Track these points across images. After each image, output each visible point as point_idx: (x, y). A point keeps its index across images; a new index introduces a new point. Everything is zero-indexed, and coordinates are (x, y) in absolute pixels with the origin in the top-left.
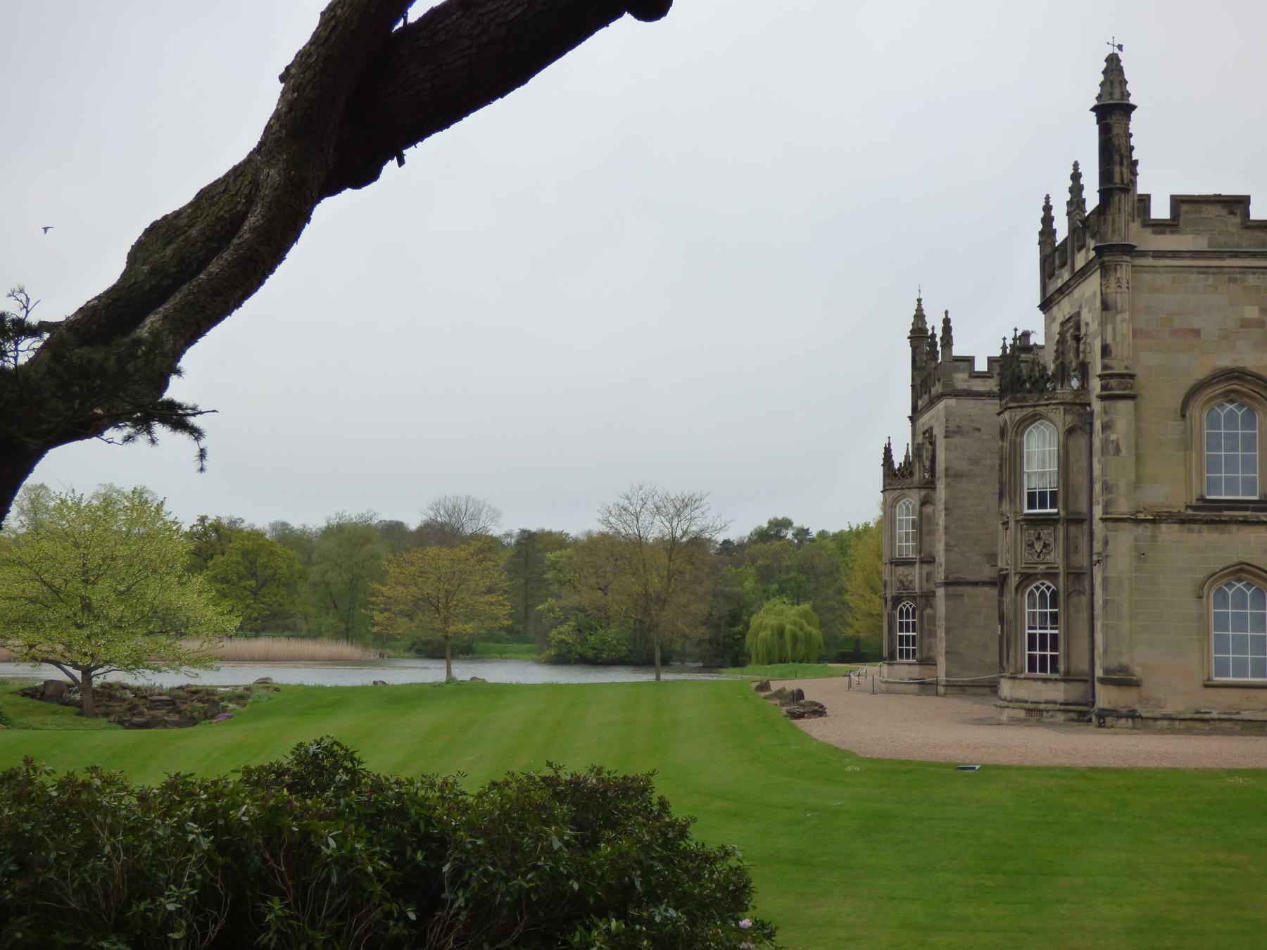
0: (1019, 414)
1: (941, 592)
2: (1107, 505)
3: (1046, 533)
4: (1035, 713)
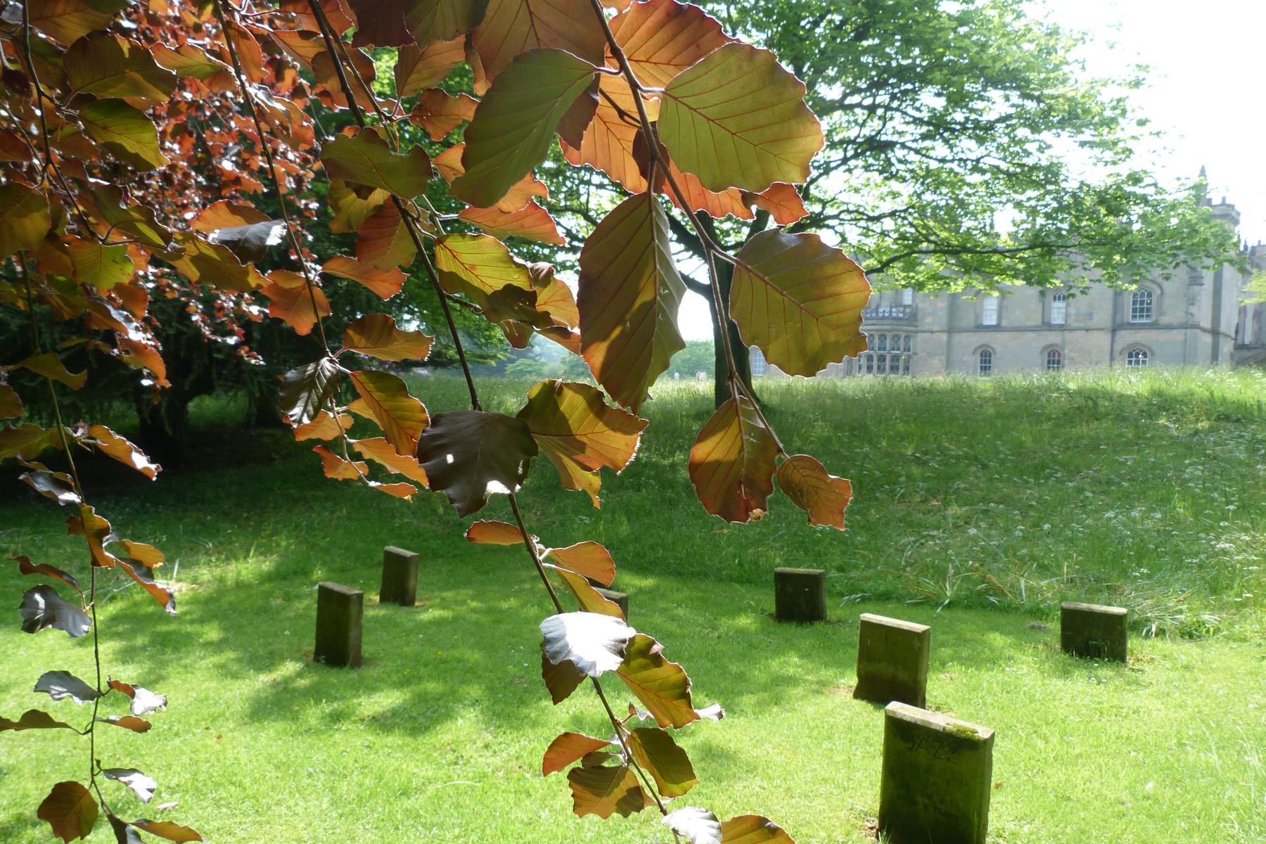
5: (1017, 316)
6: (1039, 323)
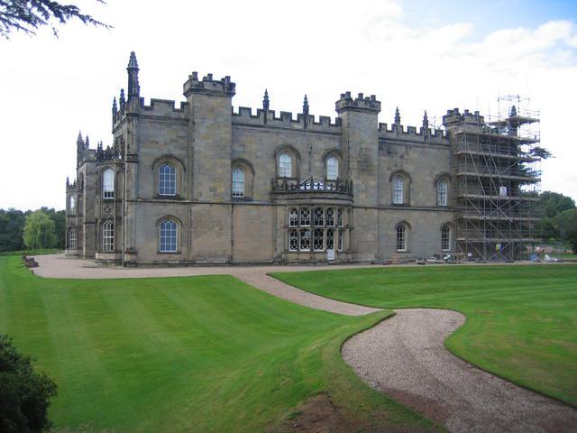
0: (103, 166)
1: (84, 226)
2: (128, 196)
3: (110, 206)
4: (105, 263)
5: (419, 198)
6: (435, 205)
